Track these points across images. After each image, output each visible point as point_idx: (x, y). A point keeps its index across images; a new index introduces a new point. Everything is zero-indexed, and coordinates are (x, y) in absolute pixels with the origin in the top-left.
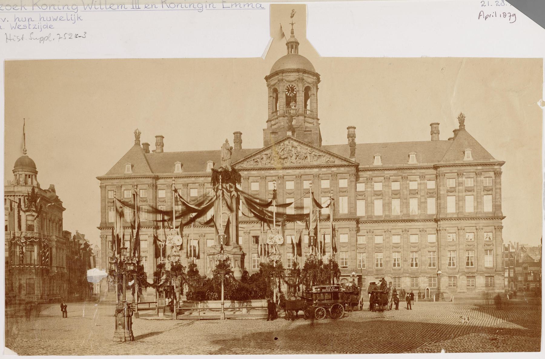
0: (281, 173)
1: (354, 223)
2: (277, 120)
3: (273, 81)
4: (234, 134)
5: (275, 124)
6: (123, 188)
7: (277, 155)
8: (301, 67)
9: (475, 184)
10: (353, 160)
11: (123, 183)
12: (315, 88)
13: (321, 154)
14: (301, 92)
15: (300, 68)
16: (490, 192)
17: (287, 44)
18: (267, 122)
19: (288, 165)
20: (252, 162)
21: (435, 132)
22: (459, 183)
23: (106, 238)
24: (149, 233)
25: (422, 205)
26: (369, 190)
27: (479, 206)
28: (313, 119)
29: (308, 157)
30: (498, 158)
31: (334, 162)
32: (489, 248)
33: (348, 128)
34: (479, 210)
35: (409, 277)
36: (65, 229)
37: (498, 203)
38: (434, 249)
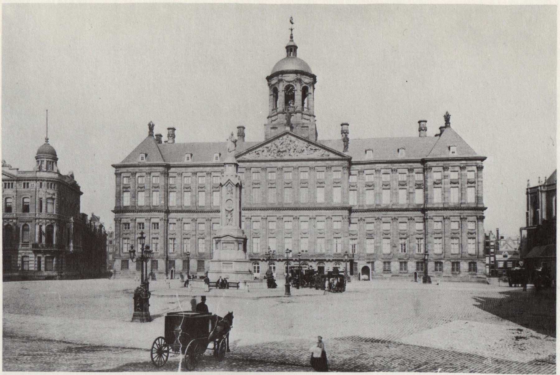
0: (280, 164)
1: (347, 212)
5: (275, 120)
6: (137, 175)
9: (460, 177)
10: (346, 154)
12: (312, 87)
13: (317, 148)
16: (473, 185)
18: (268, 118)
19: (286, 157)
22: (445, 176)
27: (463, 197)
28: (310, 116)
29: (305, 151)
31: (329, 156)
34: (463, 201)
36: (82, 211)
38: (421, 236)
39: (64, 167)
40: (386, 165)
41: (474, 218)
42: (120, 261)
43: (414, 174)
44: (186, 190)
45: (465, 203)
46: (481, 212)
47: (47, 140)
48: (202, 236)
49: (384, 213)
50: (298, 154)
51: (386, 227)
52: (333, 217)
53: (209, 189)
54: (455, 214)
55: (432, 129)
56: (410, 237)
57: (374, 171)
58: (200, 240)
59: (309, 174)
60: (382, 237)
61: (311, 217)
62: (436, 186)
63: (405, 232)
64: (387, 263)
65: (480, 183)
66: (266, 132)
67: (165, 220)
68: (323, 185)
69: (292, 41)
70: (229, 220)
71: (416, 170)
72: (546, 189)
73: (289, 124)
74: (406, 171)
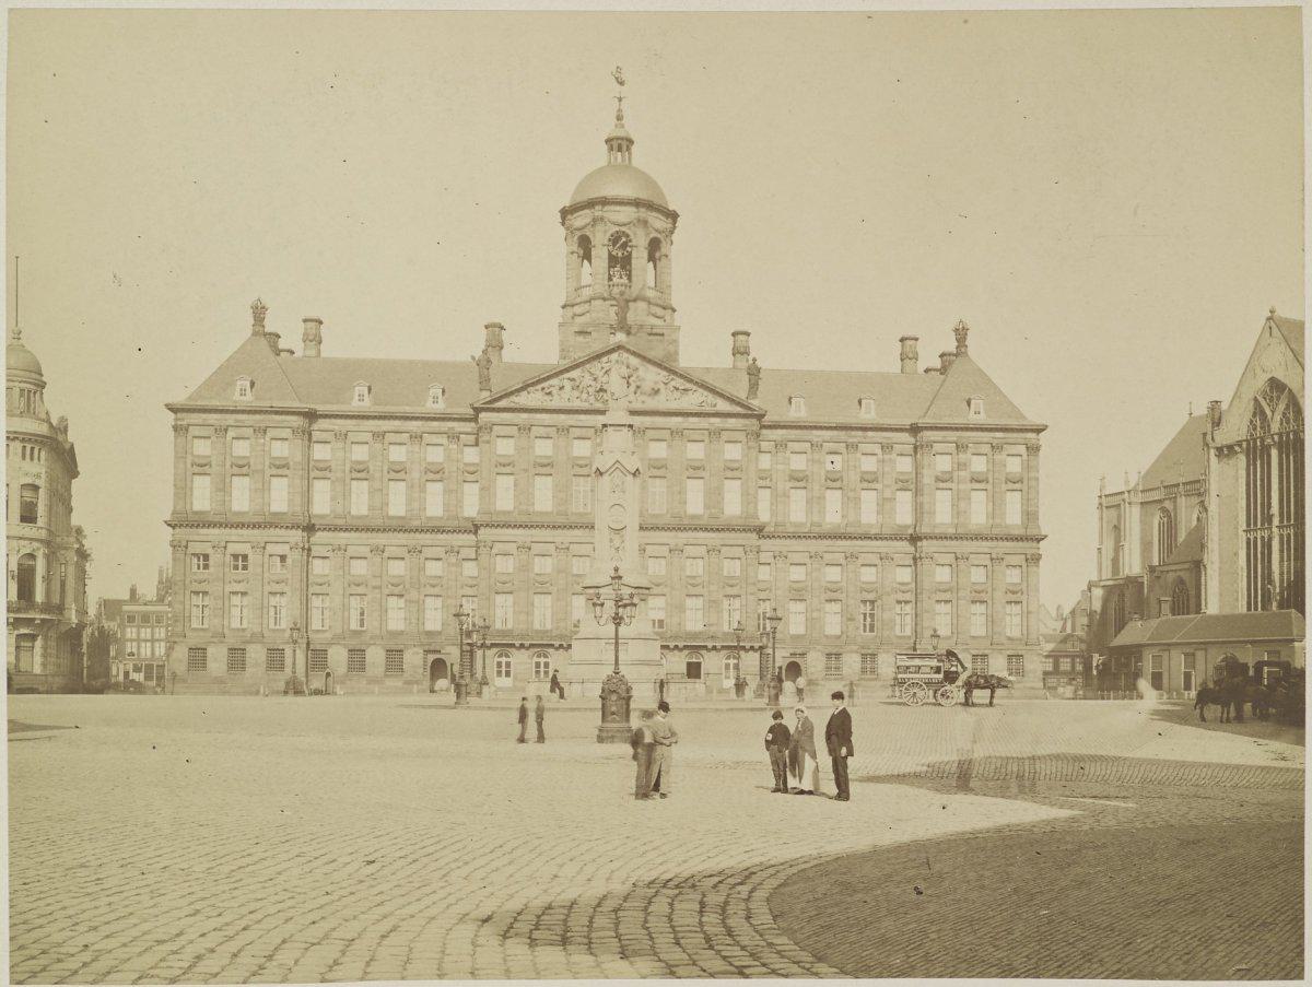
6: (231, 433)
7: (593, 383)
8: (643, 195)
10: (755, 403)
11: (231, 422)
13: (688, 386)
14: (642, 249)
15: (641, 197)
16: (1017, 486)
18: (564, 307)
20: (539, 395)
21: (911, 355)
22: (959, 464)
24: (293, 540)
25: (885, 504)
26: (780, 467)
29: (662, 390)
31: (715, 406)
33: (734, 335)
34: (998, 521)
38: (908, 597)
41: (1019, 560)
43: (894, 456)
44: (359, 475)
46: (1035, 544)
49: (829, 542)
50: (644, 398)
51: (833, 574)
52: (724, 549)
53: (416, 475)
54: (980, 550)
55: (929, 358)
58: (393, 601)
59: (669, 446)
60: (824, 597)
62: (941, 485)
64: (834, 656)
65: (1033, 483)
67: (303, 549)
68: (703, 474)
69: (623, 126)
72: (1140, 498)
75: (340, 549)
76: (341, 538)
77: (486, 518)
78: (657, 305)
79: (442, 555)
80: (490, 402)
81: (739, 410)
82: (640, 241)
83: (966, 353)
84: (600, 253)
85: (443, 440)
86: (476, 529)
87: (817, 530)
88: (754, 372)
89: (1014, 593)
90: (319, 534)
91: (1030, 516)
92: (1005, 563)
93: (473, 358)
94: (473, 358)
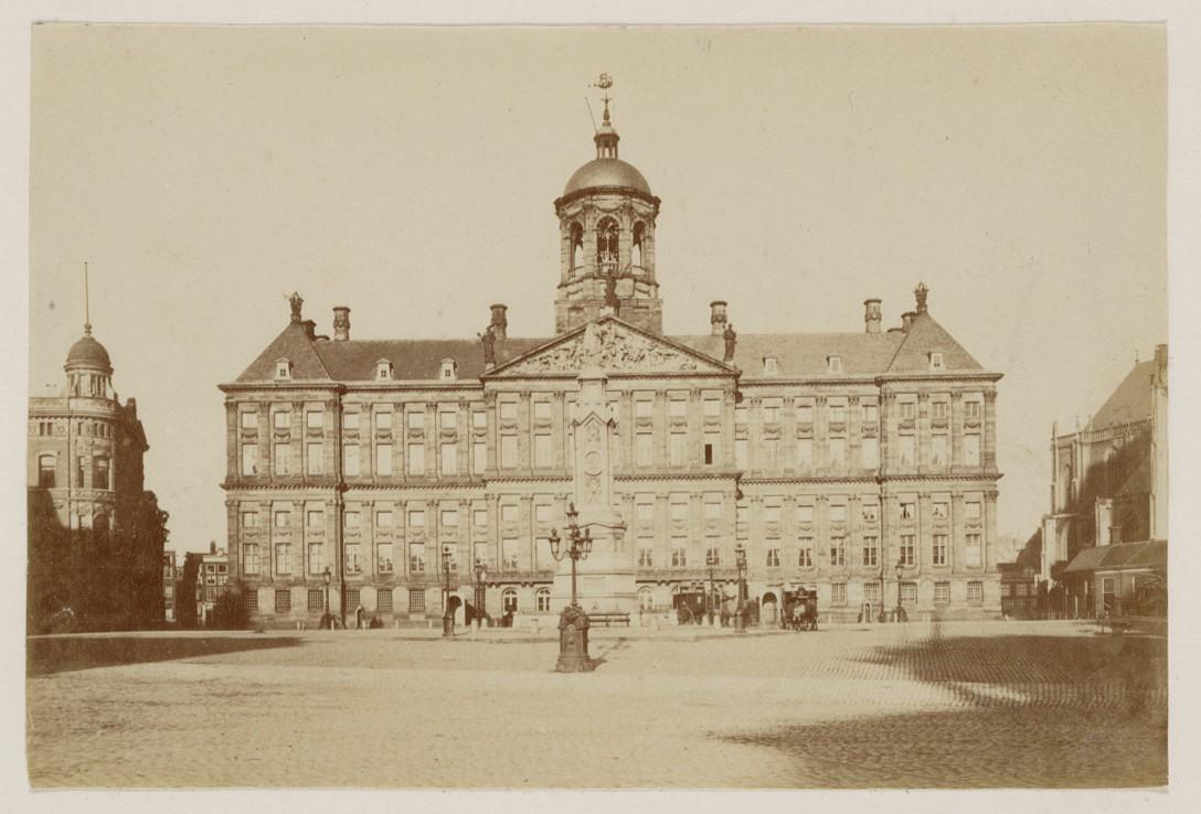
1: (732, 482)
2: (580, 284)
3: (571, 211)
4: (492, 308)
5: (576, 293)
6: (273, 408)
10: (730, 364)
11: (274, 399)
13: (670, 351)
14: (628, 232)
16: (975, 431)
17: (596, 139)
18: (559, 287)
20: (537, 364)
22: (921, 413)
23: (239, 506)
24: (328, 498)
27: (957, 455)
28: (649, 284)
29: (647, 357)
30: (989, 367)
31: (695, 368)
32: (973, 531)
34: (957, 463)
35: (828, 583)
37: (991, 450)
38: (874, 533)
39: (122, 387)
40: (805, 389)
41: (979, 496)
42: (273, 592)
43: (860, 407)
45: (960, 466)
47: (88, 328)
48: (418, 539)
50: (632, 363)
53: (432, 439)
55: (892, 318)
56: (853, 535)
57: (781, 400)
59: (655, 406)
61: (658, 494)
62: (904, 432)
63: (843, 525)
66: (558, 318)
68: (683, 429)
69: (609, 124)
70: (594, 493)
71: (863, 400)
73: (612, 300)
74: (844, 401)
75: (368, 504)
76: (369, 495)
77: (494, 474)
78: (642, 281)
79: (457, 508)
80: (492, 373)
81: (719, 371)
82: (626, 224)
83: (925, 311)
84: (590, 239)
85: (457, 409)
86: (484, 482)
87: (790, 475)
88: (730, 337)
89: (972, 526)
90: (350, 491)
91: (988, 458)
92: (964, 500)
93: (479, 335)
94: (479, 335)
